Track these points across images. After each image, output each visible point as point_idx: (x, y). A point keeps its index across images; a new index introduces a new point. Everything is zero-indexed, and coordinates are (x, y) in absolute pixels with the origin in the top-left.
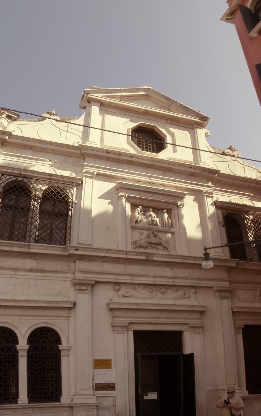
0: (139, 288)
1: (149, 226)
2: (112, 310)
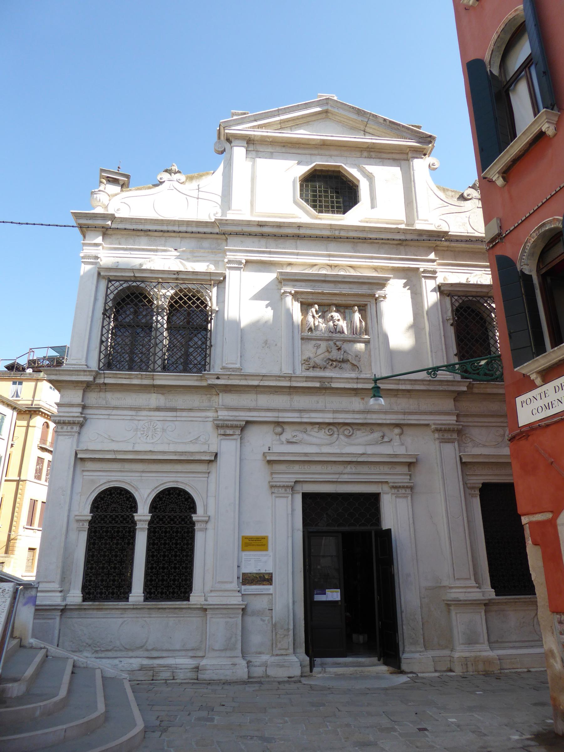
0: (312, 429)
1: (330, 334)
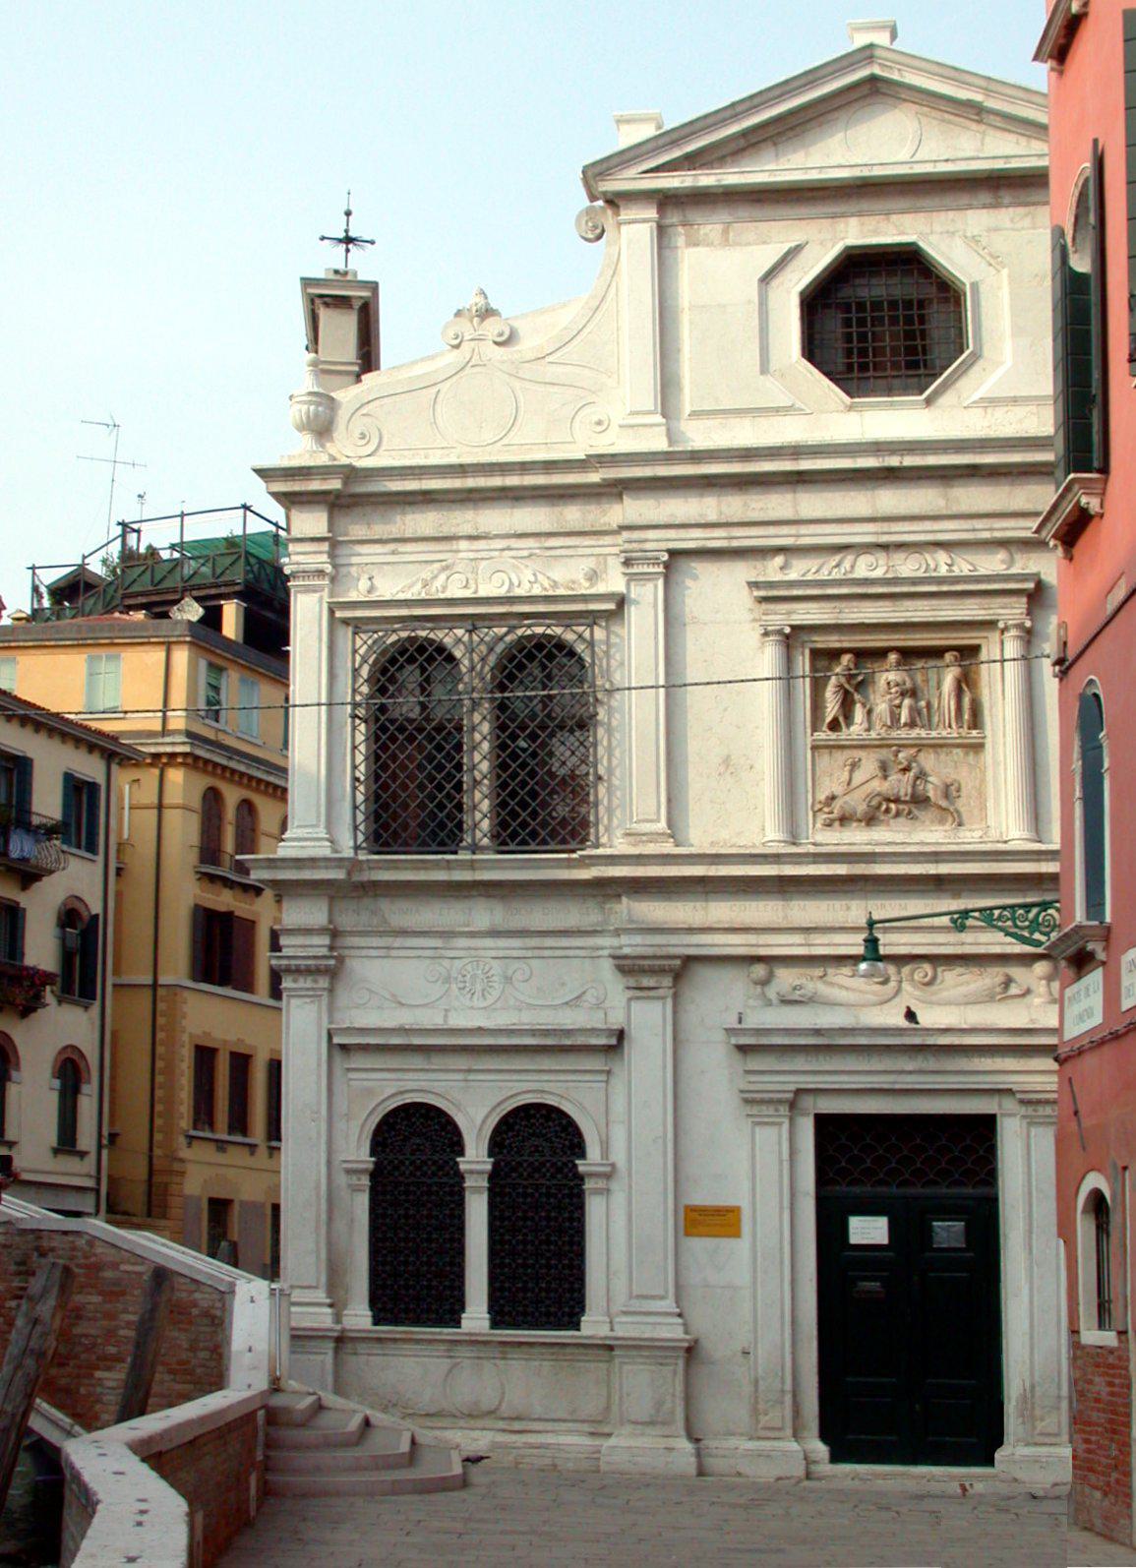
2: (743, 1049)
